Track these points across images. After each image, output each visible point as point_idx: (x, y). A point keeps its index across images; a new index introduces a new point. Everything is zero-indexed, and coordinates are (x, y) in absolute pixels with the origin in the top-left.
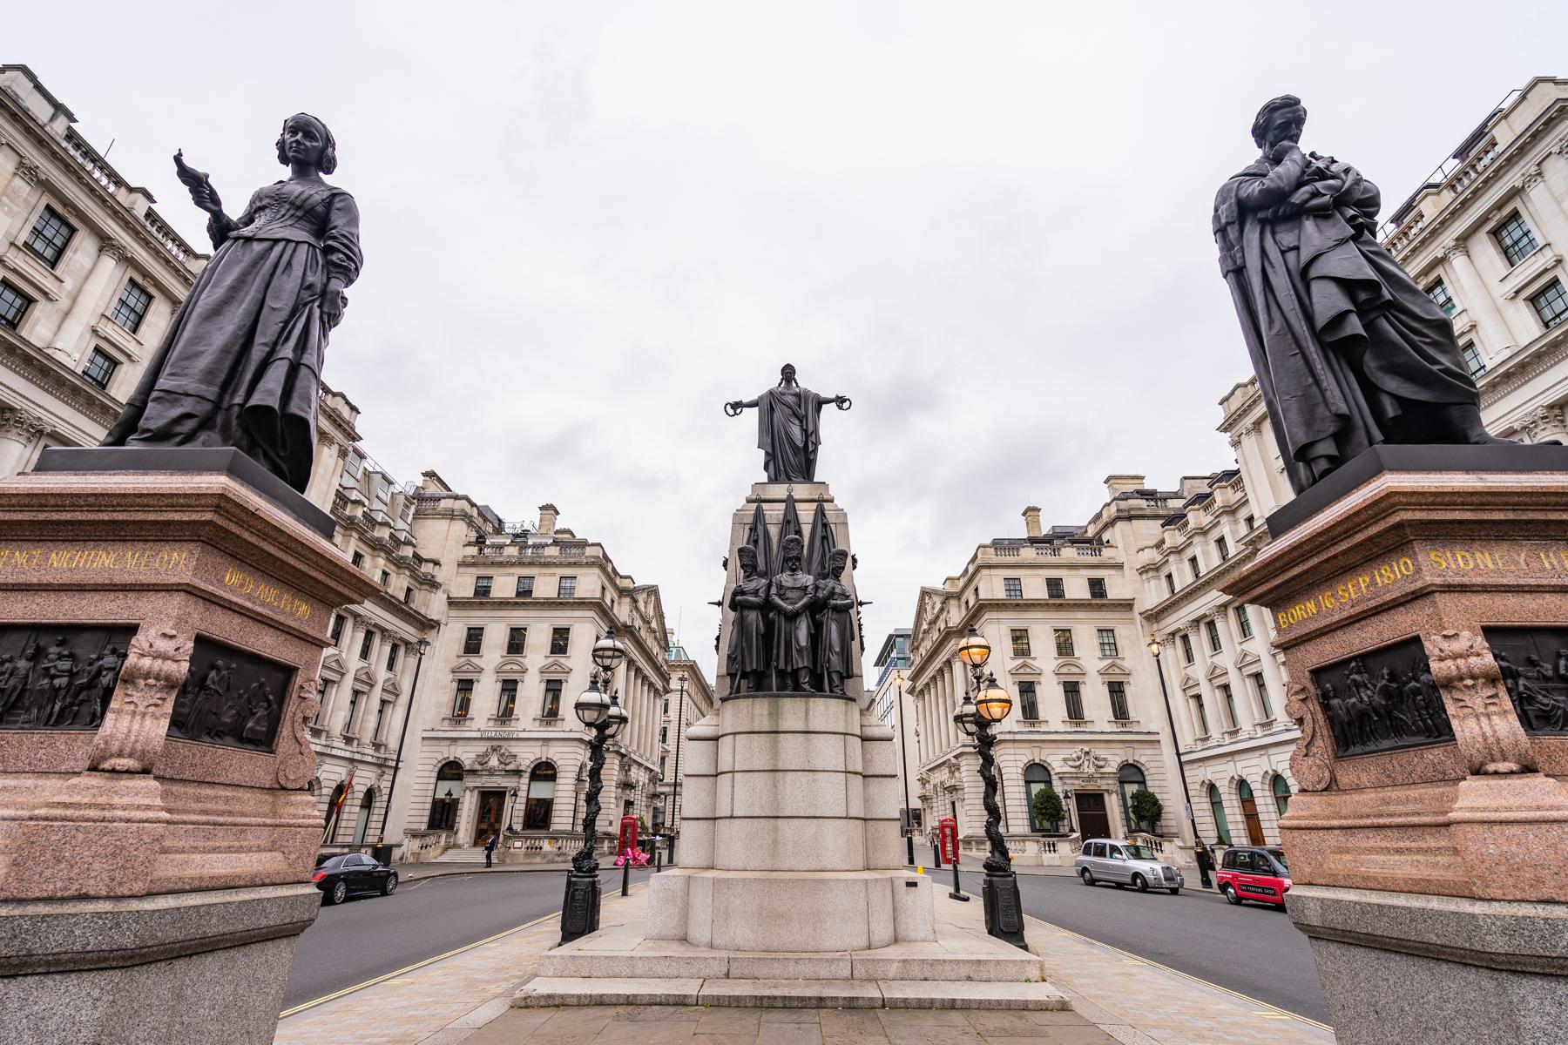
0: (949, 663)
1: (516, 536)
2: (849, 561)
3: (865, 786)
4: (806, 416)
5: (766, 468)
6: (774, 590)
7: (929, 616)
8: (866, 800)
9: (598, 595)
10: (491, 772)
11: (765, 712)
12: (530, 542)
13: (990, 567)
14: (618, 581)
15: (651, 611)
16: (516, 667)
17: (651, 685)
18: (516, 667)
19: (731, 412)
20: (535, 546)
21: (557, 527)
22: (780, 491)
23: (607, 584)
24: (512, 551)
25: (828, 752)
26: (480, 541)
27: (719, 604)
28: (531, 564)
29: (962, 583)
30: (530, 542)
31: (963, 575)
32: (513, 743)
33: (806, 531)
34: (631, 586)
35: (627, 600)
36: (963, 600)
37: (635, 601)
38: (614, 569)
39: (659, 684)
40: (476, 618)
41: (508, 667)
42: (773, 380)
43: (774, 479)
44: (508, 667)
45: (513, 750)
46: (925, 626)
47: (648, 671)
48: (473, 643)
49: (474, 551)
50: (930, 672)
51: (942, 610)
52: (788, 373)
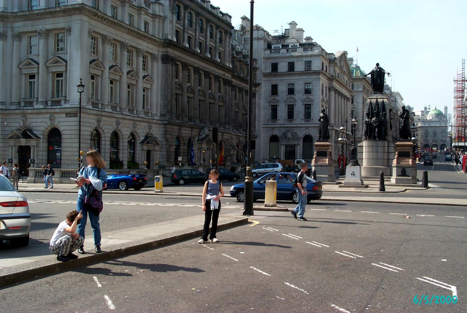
10: (289, 139)
17: (345, 97)
26: (269, 47)
32: (295, 128)
35: (332, 64)
40: (275, 80)
44: (289, 100)
45: (296, 131)
48: (274, 90)
49: (268, 52)
52: (378, 65)
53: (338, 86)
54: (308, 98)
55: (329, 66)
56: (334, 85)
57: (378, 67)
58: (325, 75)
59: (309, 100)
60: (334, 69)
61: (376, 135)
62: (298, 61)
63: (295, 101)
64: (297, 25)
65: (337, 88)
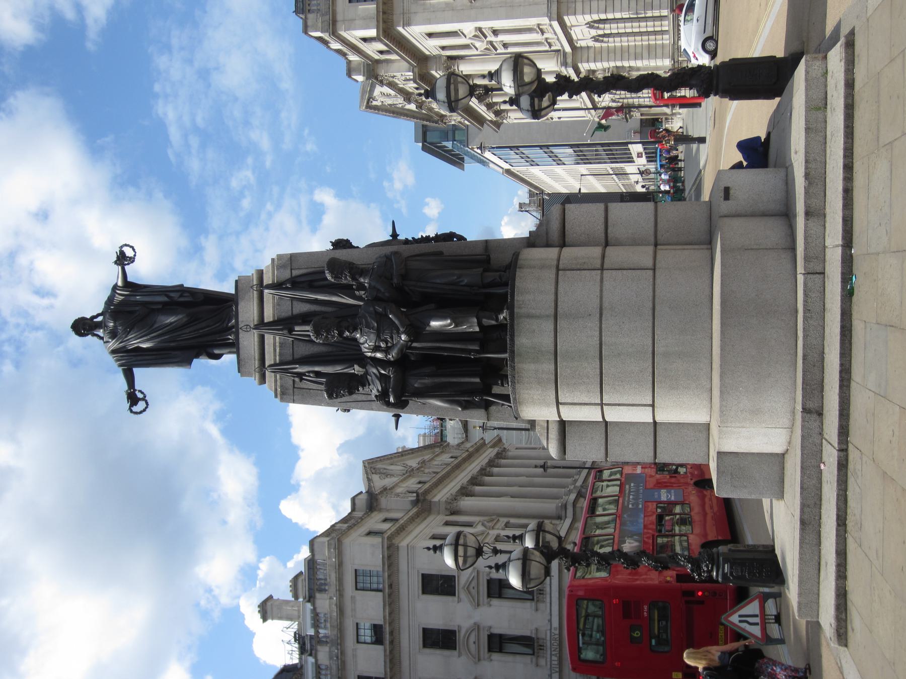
1: (302, 650)
2: (342, 254)
3: (618, 243)
4: (144, 304)
7: (399, 101)
8: (635, 242)
9: (377, 540)
11: (532, 367)
12: (311, 632)
13: (334, 22)
14: (358, 514)
15: (397, 468)
16: (473, 638)
17: (491, 463)
18: (473, 638)
19: (141, 405)
20: (316, 625)
21: (289, 597)
22: (249, 341)
23: (364, 529)
24: (323, 653)
27: (397, 417)
28: (340, 629)
29: (353, 58)
30: (311, 632)
31: (344, 55)
34: (364, 497)
35: (383, 502)
36: (377, 57)
37: (385, 490)
39: (490, 453)
41: (473, 647)
43: (234, 346)
44: (473, 647)
46: (412, 107)
47: (473, 467)
51: (392, 85)
53: (452, 484)
54: (468, 589)
55: (388, 511)
56: (444, 499)
58: (402, 529)
59: (474, 584)
60: (398, 495)
61: (471, 326)
62: (354, 610)
63: (477, 627)
64: (271, 597)
65: (458, 487)
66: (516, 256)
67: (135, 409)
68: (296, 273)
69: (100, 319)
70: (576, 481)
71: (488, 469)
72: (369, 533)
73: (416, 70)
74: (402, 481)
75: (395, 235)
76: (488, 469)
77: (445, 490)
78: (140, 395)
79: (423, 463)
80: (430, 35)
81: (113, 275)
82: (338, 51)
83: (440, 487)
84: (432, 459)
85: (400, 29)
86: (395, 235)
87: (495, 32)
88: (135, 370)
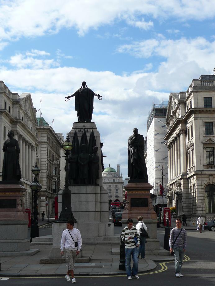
0: (178, 135)
3: (100, 204)
5: (78, 116)
6: (79, 159)
8: (101, 208)
13: (197, 92)
15: (28, 108)
17: (30, 144)
19: (67, 99)
22: (81, 125)
25: (91, 198)
29: (187, 94)
33: (88, 138)
34: (18, 98)
35: (16, 106)
37: (21, 106)
38: (9, 91)
39: (33, 143)
42: (79, 87)
50: (172, 138)
52: (84, 84)
53: (22, 131)
55: (13, 107)
56: (18, 129)
57: (84, 87)
58: (7, 115)
60: (19, 111)
65: (21, 134)
66: (98, 185)
67: (66, 98)
68: (96, 137)
69: (86, 87)
70: (24, 179)
71: (28, 144)
72: (5, 103)
73: (181, 119)
74: (23, 111)
75: (104, 156)
76: (28, 144)
77: (21, 129)
78: (69, 99)
79: (29, 118)
80: (192, 126)
81: (97, 92)
82: (188, 90)
83: (22, 127)
84: (31, 121)
85: (193, 116)
86: (104, 156)
87: (192, 150)
88: (75, 96)
